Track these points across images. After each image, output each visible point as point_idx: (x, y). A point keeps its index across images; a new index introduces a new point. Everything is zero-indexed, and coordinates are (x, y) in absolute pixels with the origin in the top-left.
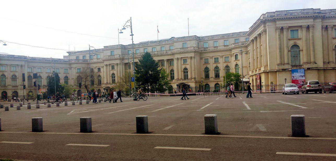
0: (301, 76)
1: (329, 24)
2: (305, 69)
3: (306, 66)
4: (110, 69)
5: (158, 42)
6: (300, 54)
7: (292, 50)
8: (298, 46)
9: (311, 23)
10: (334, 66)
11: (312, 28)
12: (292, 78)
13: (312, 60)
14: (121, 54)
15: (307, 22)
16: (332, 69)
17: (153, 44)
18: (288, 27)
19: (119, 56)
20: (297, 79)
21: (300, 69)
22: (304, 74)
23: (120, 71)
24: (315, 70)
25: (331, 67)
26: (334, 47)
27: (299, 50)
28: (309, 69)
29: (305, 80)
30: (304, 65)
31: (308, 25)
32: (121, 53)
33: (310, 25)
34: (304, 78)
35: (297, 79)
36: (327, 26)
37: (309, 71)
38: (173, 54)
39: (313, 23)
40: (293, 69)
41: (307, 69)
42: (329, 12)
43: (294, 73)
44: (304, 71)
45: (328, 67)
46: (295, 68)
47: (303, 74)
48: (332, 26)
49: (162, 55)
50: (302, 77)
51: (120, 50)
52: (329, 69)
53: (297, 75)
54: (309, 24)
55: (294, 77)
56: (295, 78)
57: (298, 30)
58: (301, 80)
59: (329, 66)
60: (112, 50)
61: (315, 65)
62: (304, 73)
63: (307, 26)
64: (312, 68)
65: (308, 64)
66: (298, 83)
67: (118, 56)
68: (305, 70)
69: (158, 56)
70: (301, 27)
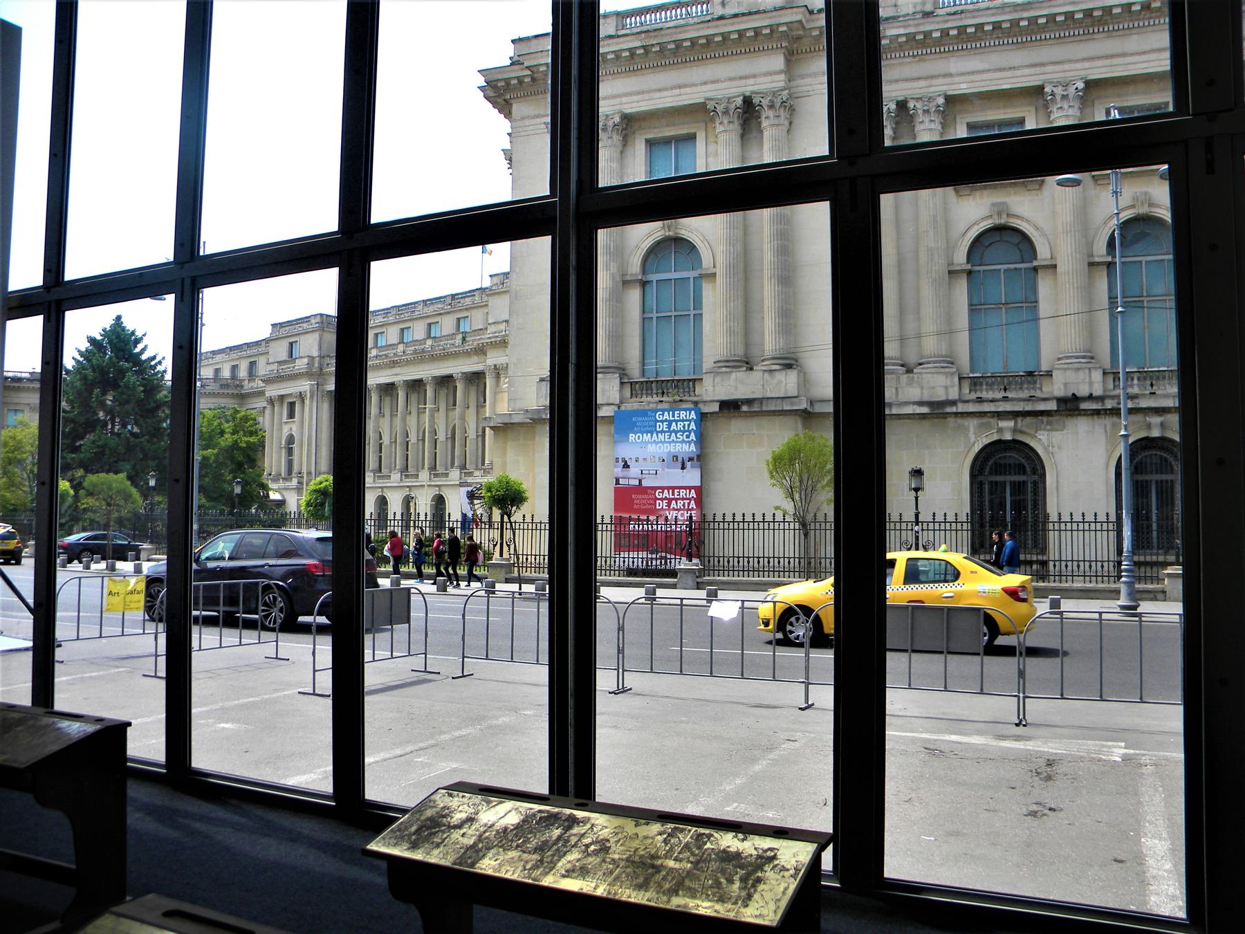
0: (675, 458)
1: (917, 93)
2: (706, 409)
3: (714, 390)
4: (281, 414)
5: (449, 300)
6: (698, 303)
7: (654, 277)
8: (692, 248)
9: (769, 79)
10: (946, 388)
11: (771, 113)
12: (619, 471)
13: (770, 342)
14: (315, 354)
15: (741, 78)
16: (925, 410)
17: (430, 310)
18: (617, 119)
19: (310, 364)
20: (645, 484)
21: (675, 406)
22: (702, 440)
23: (310, 426)
24: (777, 419)
25: (926, 399)
26: (960, 257)
27: (692, 274)
28: (730, 407)
29: (699, 490)
30: (708, 381)
31: (748, 101)
32: (316, 347)
33: (763, 94)
34: (692, 477)
35: (645, 484)
36: (902, 105)
37: (736, 426)
38: (481, 351)
39: (779, 81)
40: (632, 405)
41: (716, 407)
42: (918, 9)
43: (632, 437)
44: (693, 426)
45: (902, 398)
46: (649, 401)
47: (686, 447)
48: (941, 101)
49: (446, 356)
50: (683, 468)
51: (316, 335)
52: (909, 410)
53: (652, 449)
54: (749, 87)
55: (626, 466)
56: (634, 470)
57: (692, 138)
58: (673, 488)
59: (914, 393)
60: (292, 340)
61: (781, 376)
62: (693, 437)
63: (739, 101)
64: (749, 402)
65: (734, 375)
66: (653, 511)
67: (306, 360)
68: (703, 417)
69: (434, 358)
70: (702, 112)
